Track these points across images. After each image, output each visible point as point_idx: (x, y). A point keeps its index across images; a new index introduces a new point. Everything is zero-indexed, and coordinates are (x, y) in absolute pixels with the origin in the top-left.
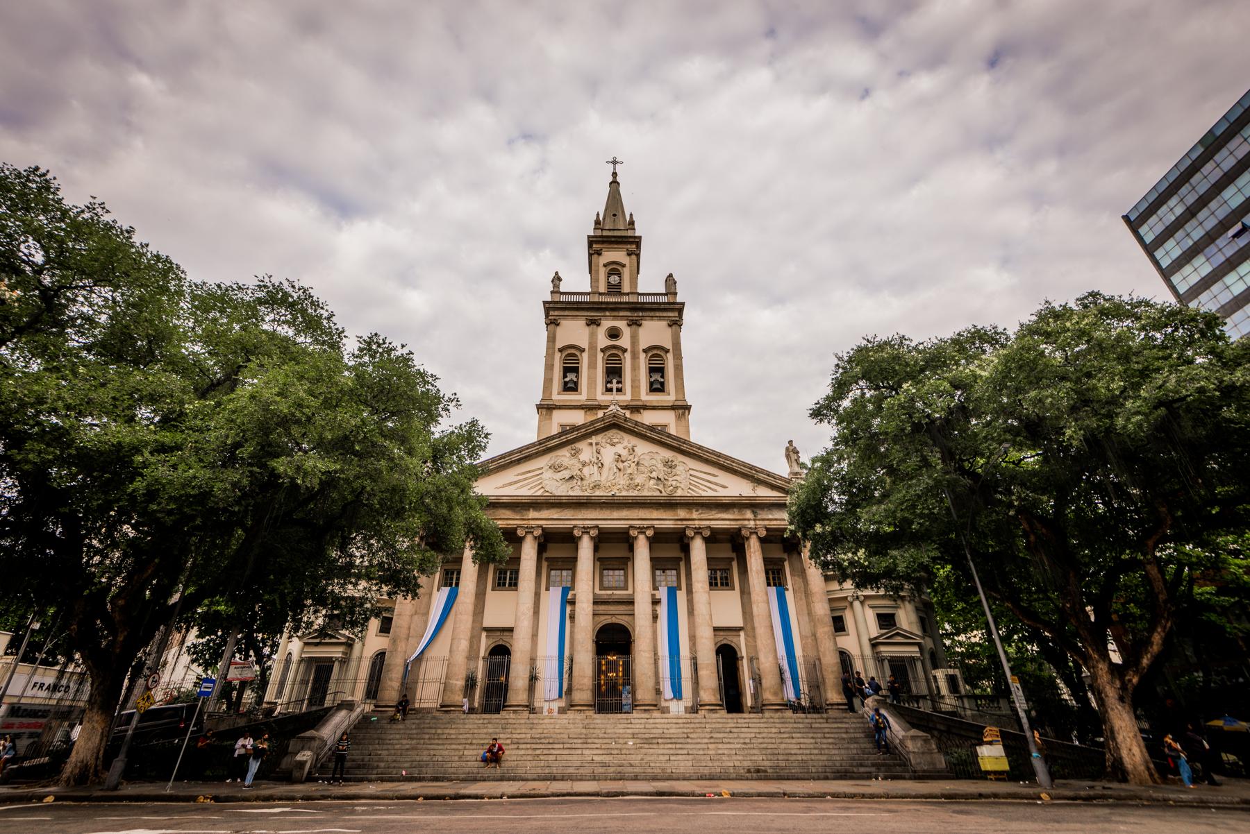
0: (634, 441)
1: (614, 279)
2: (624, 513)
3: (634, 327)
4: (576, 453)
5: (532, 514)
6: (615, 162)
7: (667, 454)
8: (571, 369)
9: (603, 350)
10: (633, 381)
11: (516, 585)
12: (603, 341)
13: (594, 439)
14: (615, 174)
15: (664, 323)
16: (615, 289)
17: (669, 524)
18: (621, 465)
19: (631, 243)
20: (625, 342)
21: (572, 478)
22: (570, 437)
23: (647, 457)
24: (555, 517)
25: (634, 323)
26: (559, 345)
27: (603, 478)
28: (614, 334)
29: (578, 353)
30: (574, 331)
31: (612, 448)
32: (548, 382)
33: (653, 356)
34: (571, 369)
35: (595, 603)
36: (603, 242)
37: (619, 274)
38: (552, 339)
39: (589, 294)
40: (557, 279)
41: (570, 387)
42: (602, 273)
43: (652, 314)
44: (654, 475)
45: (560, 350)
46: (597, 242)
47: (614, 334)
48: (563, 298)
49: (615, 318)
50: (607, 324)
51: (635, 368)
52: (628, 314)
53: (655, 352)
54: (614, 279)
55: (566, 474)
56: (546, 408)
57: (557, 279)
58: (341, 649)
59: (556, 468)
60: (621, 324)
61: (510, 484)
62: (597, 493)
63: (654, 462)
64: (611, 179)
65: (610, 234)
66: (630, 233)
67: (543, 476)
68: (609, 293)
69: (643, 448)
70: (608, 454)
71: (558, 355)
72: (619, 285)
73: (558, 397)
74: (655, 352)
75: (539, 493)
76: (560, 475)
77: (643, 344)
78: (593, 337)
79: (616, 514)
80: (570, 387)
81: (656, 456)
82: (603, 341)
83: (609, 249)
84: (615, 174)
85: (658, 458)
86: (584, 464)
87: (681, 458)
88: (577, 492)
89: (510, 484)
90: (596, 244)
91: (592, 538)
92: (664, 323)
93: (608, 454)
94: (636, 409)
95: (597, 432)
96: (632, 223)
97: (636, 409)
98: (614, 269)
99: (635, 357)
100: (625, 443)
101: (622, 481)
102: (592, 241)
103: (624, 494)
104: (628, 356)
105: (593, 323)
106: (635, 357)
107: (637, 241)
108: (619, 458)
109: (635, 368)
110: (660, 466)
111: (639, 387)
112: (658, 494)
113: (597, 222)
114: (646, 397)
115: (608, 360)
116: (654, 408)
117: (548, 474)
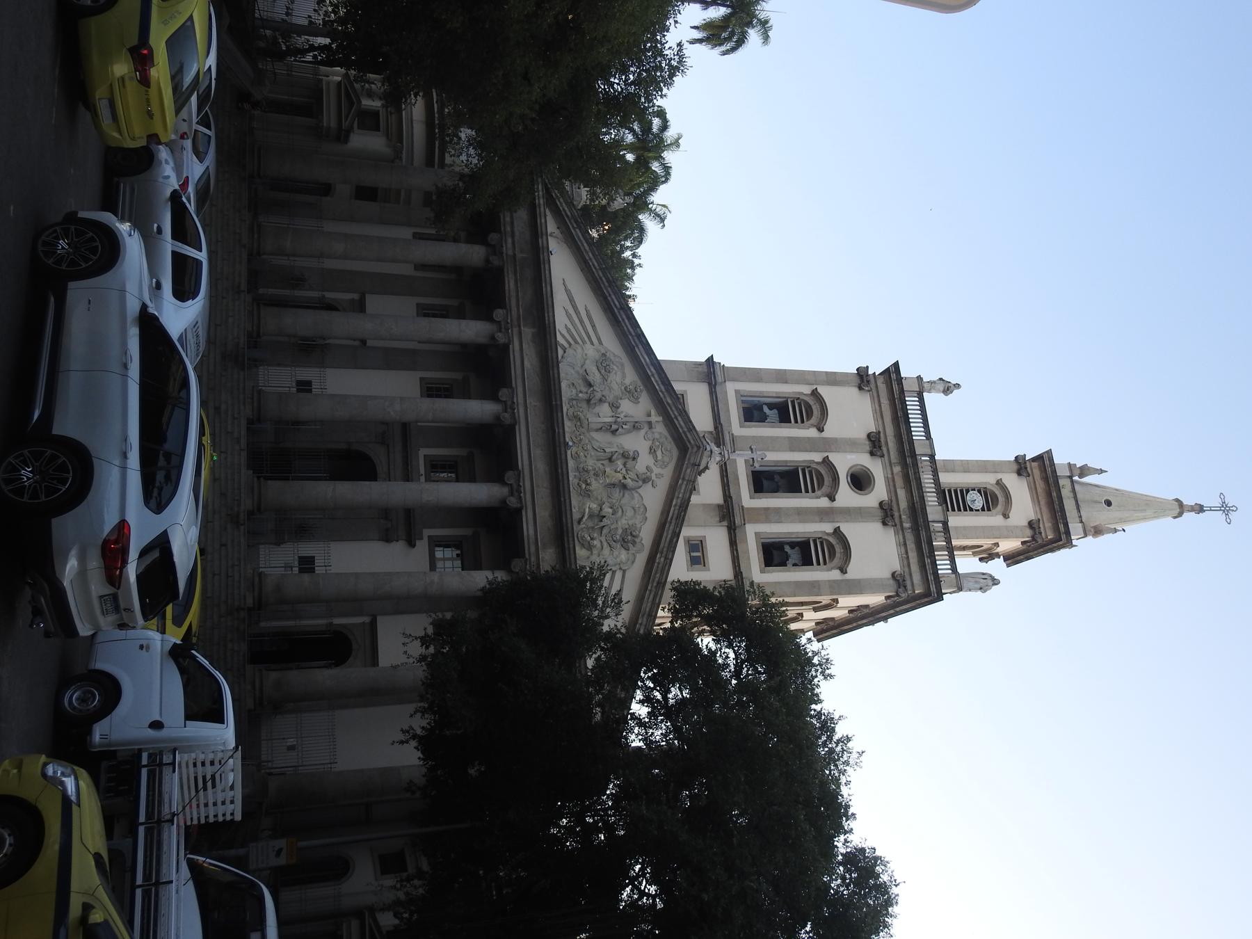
0: (663, 485)
1: (976, 500)
2: (541, 466)
3: (879, 513)
4: (631, 394)
5: (528, 332)
6: (1225, 509)
7: (647, 534)
8: (784, 411)
9: (826, 462)
10: (778, 511)
11: (429, 396)
12: (844, 463)
13: (655, 418)
14: (1200, 509)
15: (896, 566)
16: (954, 499)
17: (528, 529)
18: (620, 463)
19: (1056, 528)
20: (846, 496)
21: (590, 385)
22: (655, 379)
23: (636, 503)
24: (526, 363)
25: (886, 513)
26: (824, 391)
27: (594, 435)
28: (860, 481)
29: (814, 420)
30: (852, 417)
31: (647, 451)
32: (756, 375)
33: (831, 547)
34: (784, 411)
35: (405, 426)
36: (1045, 479)
37: (987, 508)
38: (833, 379)
39: (932, 456)
40: (948, 388)
41: (753, 412)
42: (988, 479)
43: (911, 546)
44: (607, 510)
45: (815, 393)
46: (1043, 469)
47: (860, 481)
48: (912, 403)
49: (891, 483)
50: (877, 469)
51: (802, 515)
52: (903, 504)
53: (838, 549)
54: (976, 500)
55: (595, 376)
56: (710, 372)
57: (948, 388)
58: (333, 124)
59: (604, 363)
60: (879, 492)
61: (571, 300)
62: (567, 424)
63: (630, 513)
64: (1188, 501)
65: (1066, 492)
66: (1075, 527)
67: (588, 345)
68: (941, 493)
69: (653, 498)
70: (635, 442)
71: (807, 390)
72: (966, 508)
73: (730, 390)
74: (838, 549)
75: (559, 338)
76: (593, 369)
77: (848, 529)
78: (848, 445)
79: (538, 453)
80: (753, 412)
81: (639, 517)
82: (844, 463)
83: (1033, 489)
84: (1200, 509)
85: (637, 521)
86: (614, 406)
87: (641, 559)
88: (567, 392)
89: (571, 300)
90: (1039, 471)
91: (498, 418)
92: (896, 566)
93: (635, 442)
94: (728, 513)
95: (669, 422)
96: (1098, 531)
97: (728, 513)
98: (994, 499)
99: (823, 515)
100: (656, 470)
101: (591, 463)
102: (1044, 460)
103: (571, 463)
104: (824, 502)
105: (875, 444)
106: (823, 515)
107: (1061, 539)
108: (629, 457)
109: (802, 515)
110: (623, 522)
111: (768, 520)
112: (576, 516)
113: (1084, 471)
114: (752, 533)
115: (808, 468)
116: (733, 543)
117: (591, 351)
